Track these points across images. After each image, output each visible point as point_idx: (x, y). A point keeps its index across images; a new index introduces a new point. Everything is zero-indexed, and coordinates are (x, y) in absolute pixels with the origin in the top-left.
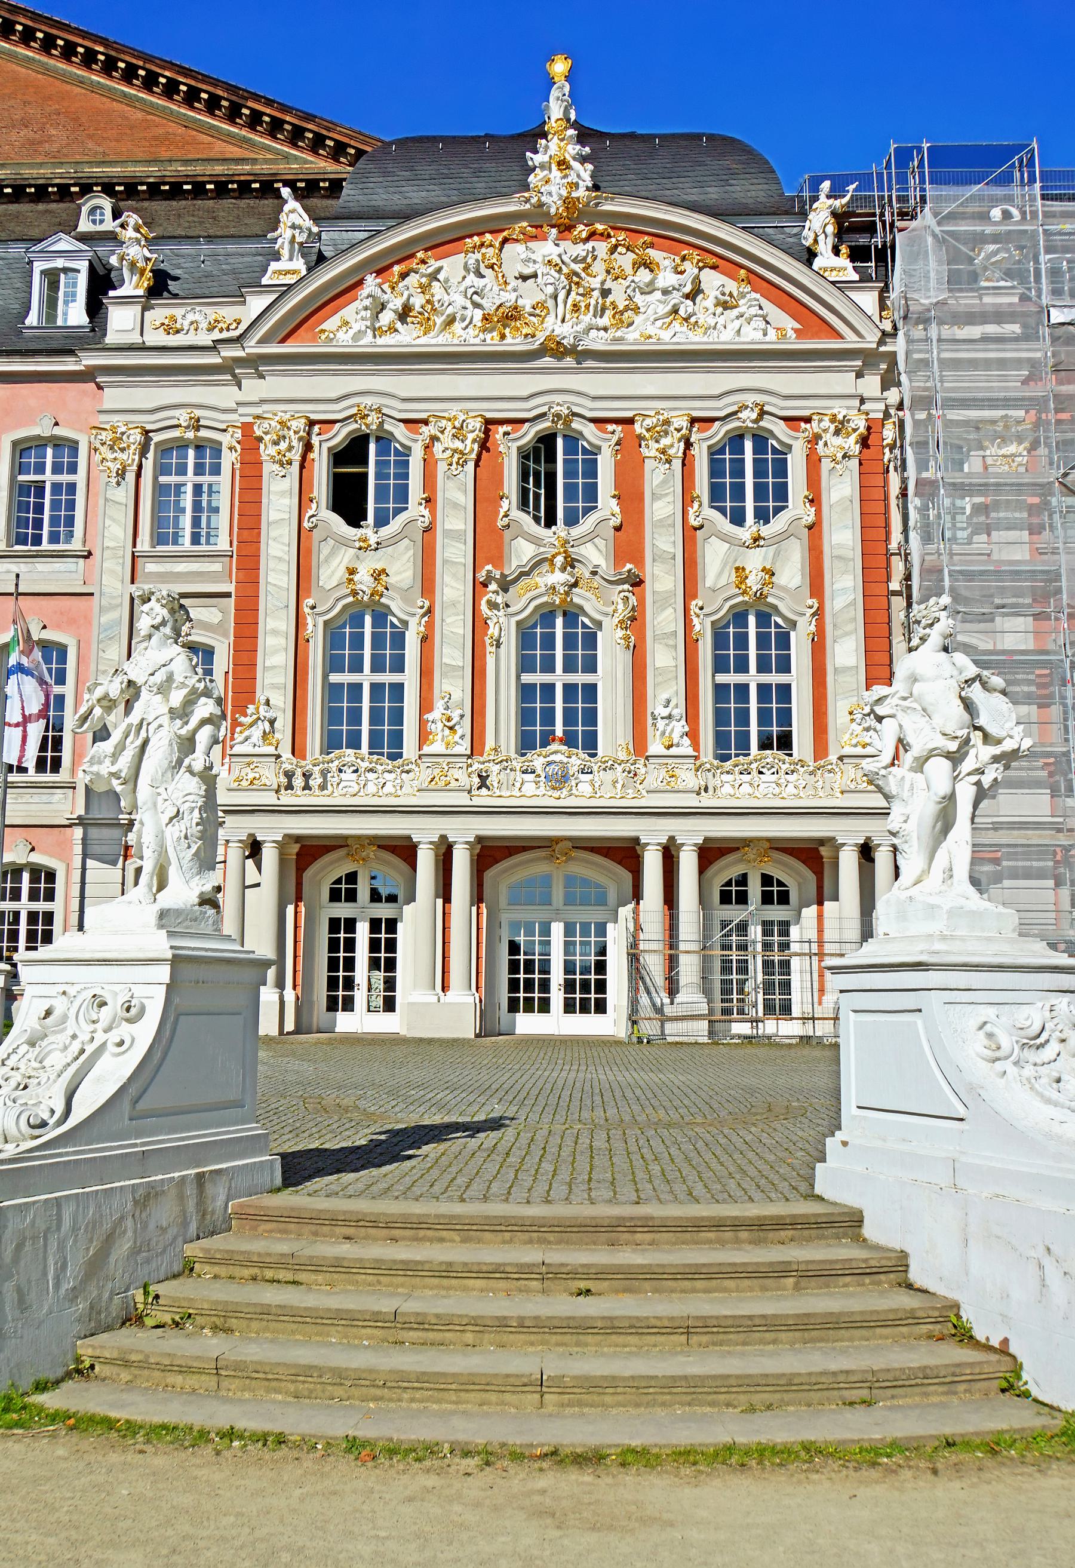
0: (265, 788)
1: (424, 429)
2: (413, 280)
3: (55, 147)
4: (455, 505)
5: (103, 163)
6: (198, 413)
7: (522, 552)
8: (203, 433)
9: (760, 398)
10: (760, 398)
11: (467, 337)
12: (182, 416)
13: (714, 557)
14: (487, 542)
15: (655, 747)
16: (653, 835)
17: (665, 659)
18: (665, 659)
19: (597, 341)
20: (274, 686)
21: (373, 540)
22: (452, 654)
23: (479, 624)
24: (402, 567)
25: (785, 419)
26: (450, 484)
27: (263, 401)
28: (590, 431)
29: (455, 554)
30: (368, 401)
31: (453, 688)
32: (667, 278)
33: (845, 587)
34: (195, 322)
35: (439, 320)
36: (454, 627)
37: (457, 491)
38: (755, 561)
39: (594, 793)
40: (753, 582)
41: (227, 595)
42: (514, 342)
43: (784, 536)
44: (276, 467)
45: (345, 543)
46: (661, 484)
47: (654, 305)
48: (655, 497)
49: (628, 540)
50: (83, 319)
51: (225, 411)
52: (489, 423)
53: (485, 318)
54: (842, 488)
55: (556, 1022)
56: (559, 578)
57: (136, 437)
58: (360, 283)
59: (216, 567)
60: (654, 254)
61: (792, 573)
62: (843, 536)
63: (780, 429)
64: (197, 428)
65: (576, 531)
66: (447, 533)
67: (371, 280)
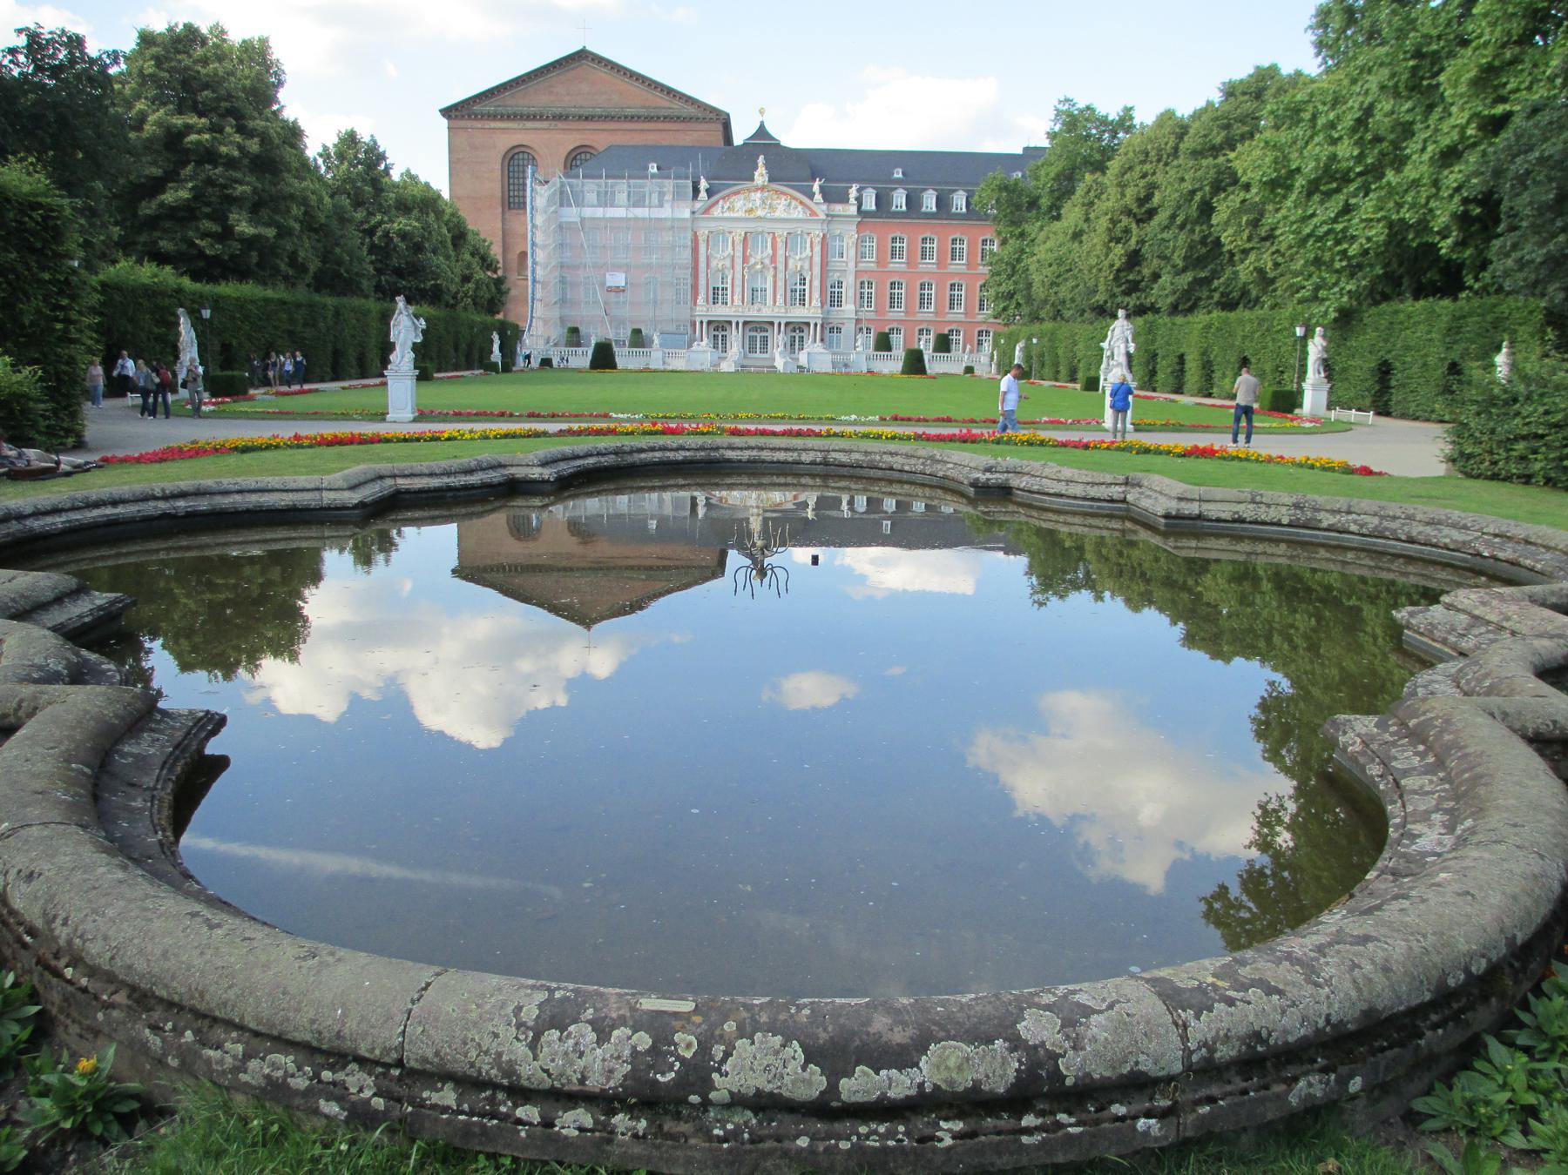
7: (752, 261)
13: (791, 262)
14: (745, 259)
17: (780, 284)
18: (780, 284)
22: (738, 282)
24: (728, 263)
29: (739, 261)
31: (738, 290)
33: (817, 270)
36: (738, 276)
37: (739, 248)
39: (765, 312)
46: (780, 245)
47: (781, 207)
49: (773, 259)
54: (817, 249)
55: (758, 355)
61: (807, 266)
62: (817, 259)
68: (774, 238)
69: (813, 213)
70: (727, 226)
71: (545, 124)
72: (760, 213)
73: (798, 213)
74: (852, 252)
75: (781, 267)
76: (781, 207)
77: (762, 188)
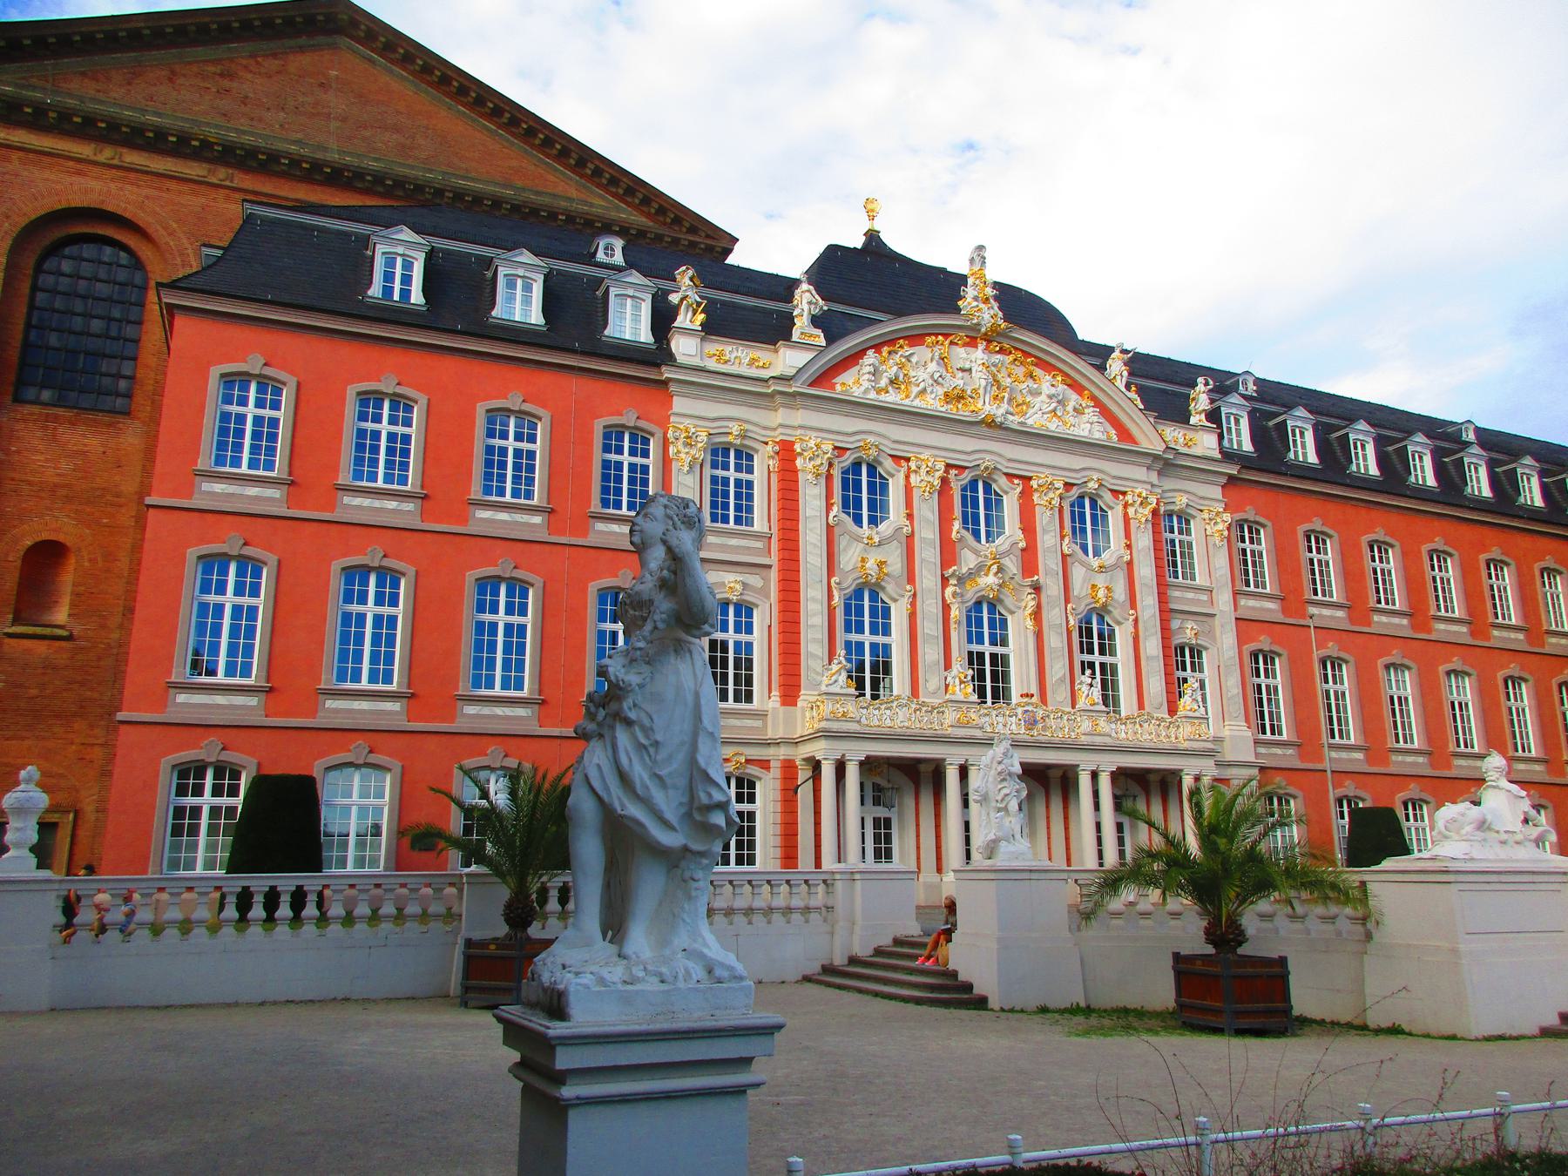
0: (852, 720)
1: (903, 463)
2: (897, 358)
3: (423, 155)
4: (928, 521)
5: (463, 178)
6: (747, 426)
7: (968, 560)
8: (747, 442)
9: (1101, 476)
10: (1101, 476)
11: (932, 403)
12: (735, 428)
13: (1078, 573)
14: (948, 553)
15: (1081, 704)
16: (1085, 763)
18: (1055, 642)
19: (1013, 421)
20: (814, 640)
21: (876, 539)
23: (946, 608)
25: (1112, 491)
26: (924, 506)
27: (801, 427)
28: (1003, 481)
29: (928, 555)
30: (871, 439)
32: (1046, 388)
34: (739, 357)
35: (915, 390)
37: (927, 511)
38: (1101, 581)
40: (1101, 594)
41: (770, 567)
42: (961, 412)
43: (1115, 566)
44: (810, 476)
45: (858, 539)
47: (1041, 402)
48: (1045, 531)
50: (645, 336)
51: (765, 428)
52: (948, 466)
53: (946, 395)
54: (1144, 540)
56: (989, 580)
57: (703, 436)
58: (862, 353)
59: (759, 545)
60: (1038, 372)
61: (1120, 593)
62: (1146, 571)
63: (1108, 496)
64: (744, 437)
65: (992, 547)
66: (923, 540)
67: (870, 352)
68: (1026, 494)
69: (1124, 434)
70: (888, 436)
71: (195, 170)
72: (987, 407)
73: (1089, 426)
74: (1221, 561)
75: (1053, 588)
76: (1041, 402)
77: (990, 338)
